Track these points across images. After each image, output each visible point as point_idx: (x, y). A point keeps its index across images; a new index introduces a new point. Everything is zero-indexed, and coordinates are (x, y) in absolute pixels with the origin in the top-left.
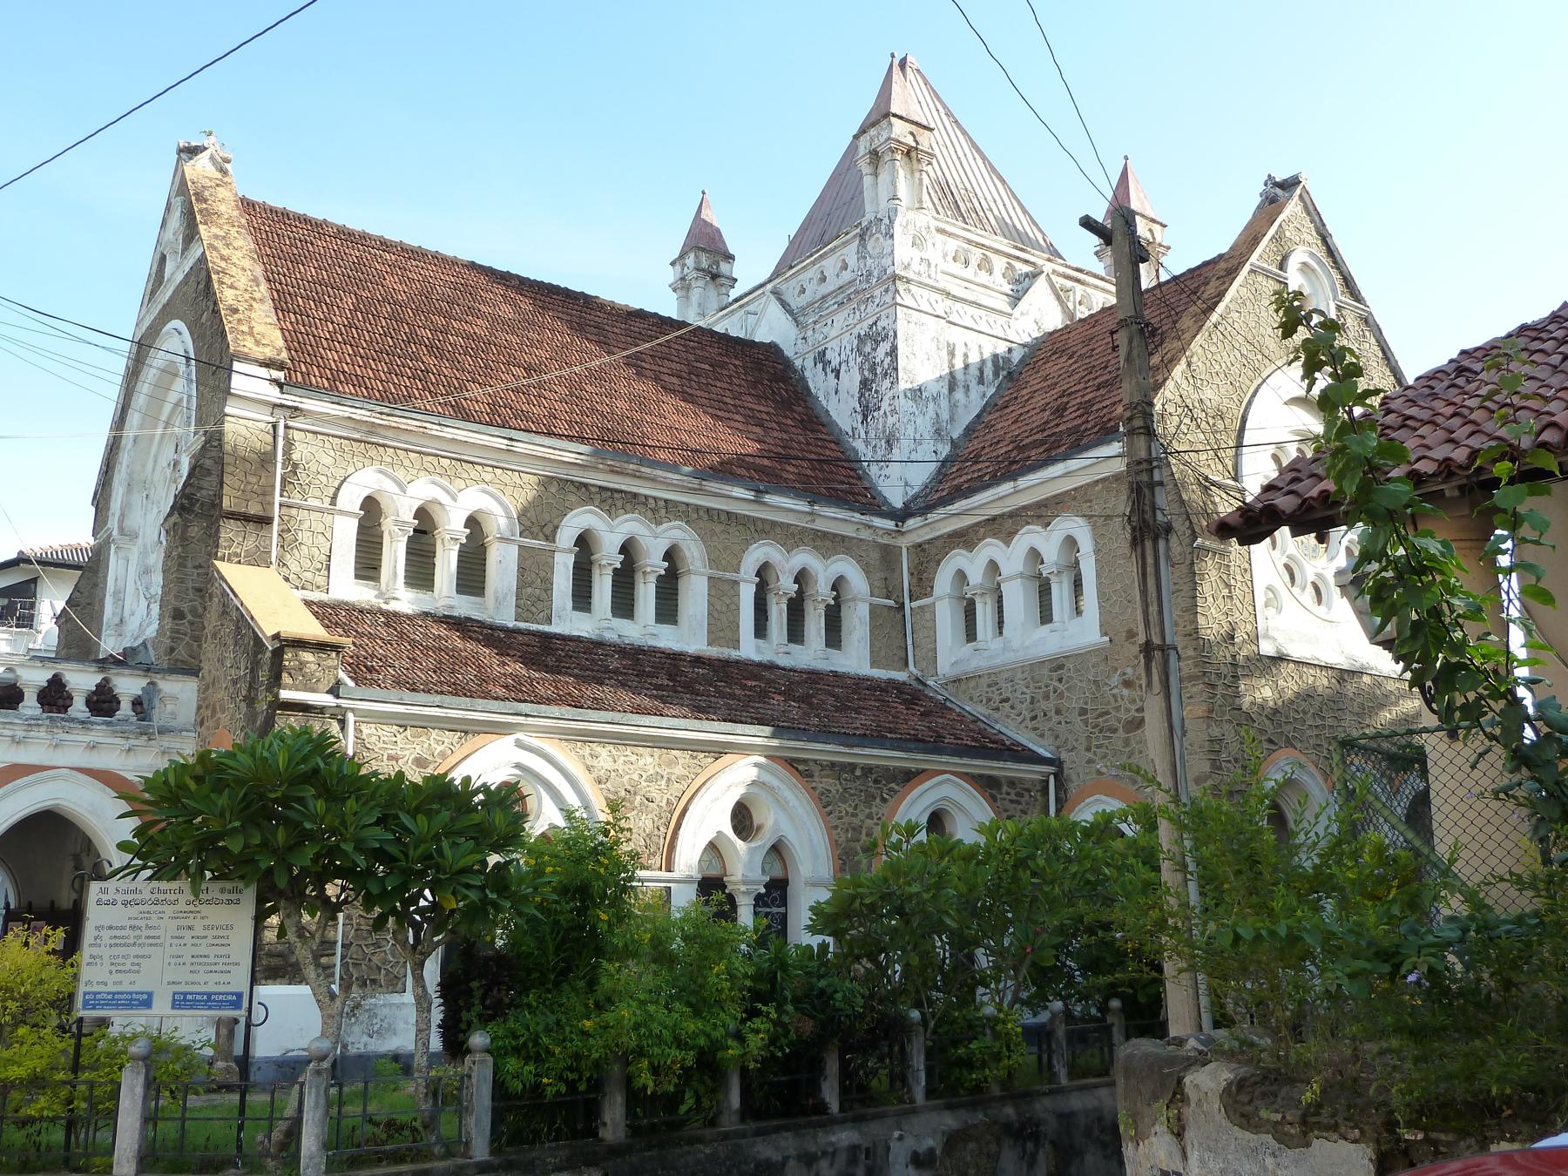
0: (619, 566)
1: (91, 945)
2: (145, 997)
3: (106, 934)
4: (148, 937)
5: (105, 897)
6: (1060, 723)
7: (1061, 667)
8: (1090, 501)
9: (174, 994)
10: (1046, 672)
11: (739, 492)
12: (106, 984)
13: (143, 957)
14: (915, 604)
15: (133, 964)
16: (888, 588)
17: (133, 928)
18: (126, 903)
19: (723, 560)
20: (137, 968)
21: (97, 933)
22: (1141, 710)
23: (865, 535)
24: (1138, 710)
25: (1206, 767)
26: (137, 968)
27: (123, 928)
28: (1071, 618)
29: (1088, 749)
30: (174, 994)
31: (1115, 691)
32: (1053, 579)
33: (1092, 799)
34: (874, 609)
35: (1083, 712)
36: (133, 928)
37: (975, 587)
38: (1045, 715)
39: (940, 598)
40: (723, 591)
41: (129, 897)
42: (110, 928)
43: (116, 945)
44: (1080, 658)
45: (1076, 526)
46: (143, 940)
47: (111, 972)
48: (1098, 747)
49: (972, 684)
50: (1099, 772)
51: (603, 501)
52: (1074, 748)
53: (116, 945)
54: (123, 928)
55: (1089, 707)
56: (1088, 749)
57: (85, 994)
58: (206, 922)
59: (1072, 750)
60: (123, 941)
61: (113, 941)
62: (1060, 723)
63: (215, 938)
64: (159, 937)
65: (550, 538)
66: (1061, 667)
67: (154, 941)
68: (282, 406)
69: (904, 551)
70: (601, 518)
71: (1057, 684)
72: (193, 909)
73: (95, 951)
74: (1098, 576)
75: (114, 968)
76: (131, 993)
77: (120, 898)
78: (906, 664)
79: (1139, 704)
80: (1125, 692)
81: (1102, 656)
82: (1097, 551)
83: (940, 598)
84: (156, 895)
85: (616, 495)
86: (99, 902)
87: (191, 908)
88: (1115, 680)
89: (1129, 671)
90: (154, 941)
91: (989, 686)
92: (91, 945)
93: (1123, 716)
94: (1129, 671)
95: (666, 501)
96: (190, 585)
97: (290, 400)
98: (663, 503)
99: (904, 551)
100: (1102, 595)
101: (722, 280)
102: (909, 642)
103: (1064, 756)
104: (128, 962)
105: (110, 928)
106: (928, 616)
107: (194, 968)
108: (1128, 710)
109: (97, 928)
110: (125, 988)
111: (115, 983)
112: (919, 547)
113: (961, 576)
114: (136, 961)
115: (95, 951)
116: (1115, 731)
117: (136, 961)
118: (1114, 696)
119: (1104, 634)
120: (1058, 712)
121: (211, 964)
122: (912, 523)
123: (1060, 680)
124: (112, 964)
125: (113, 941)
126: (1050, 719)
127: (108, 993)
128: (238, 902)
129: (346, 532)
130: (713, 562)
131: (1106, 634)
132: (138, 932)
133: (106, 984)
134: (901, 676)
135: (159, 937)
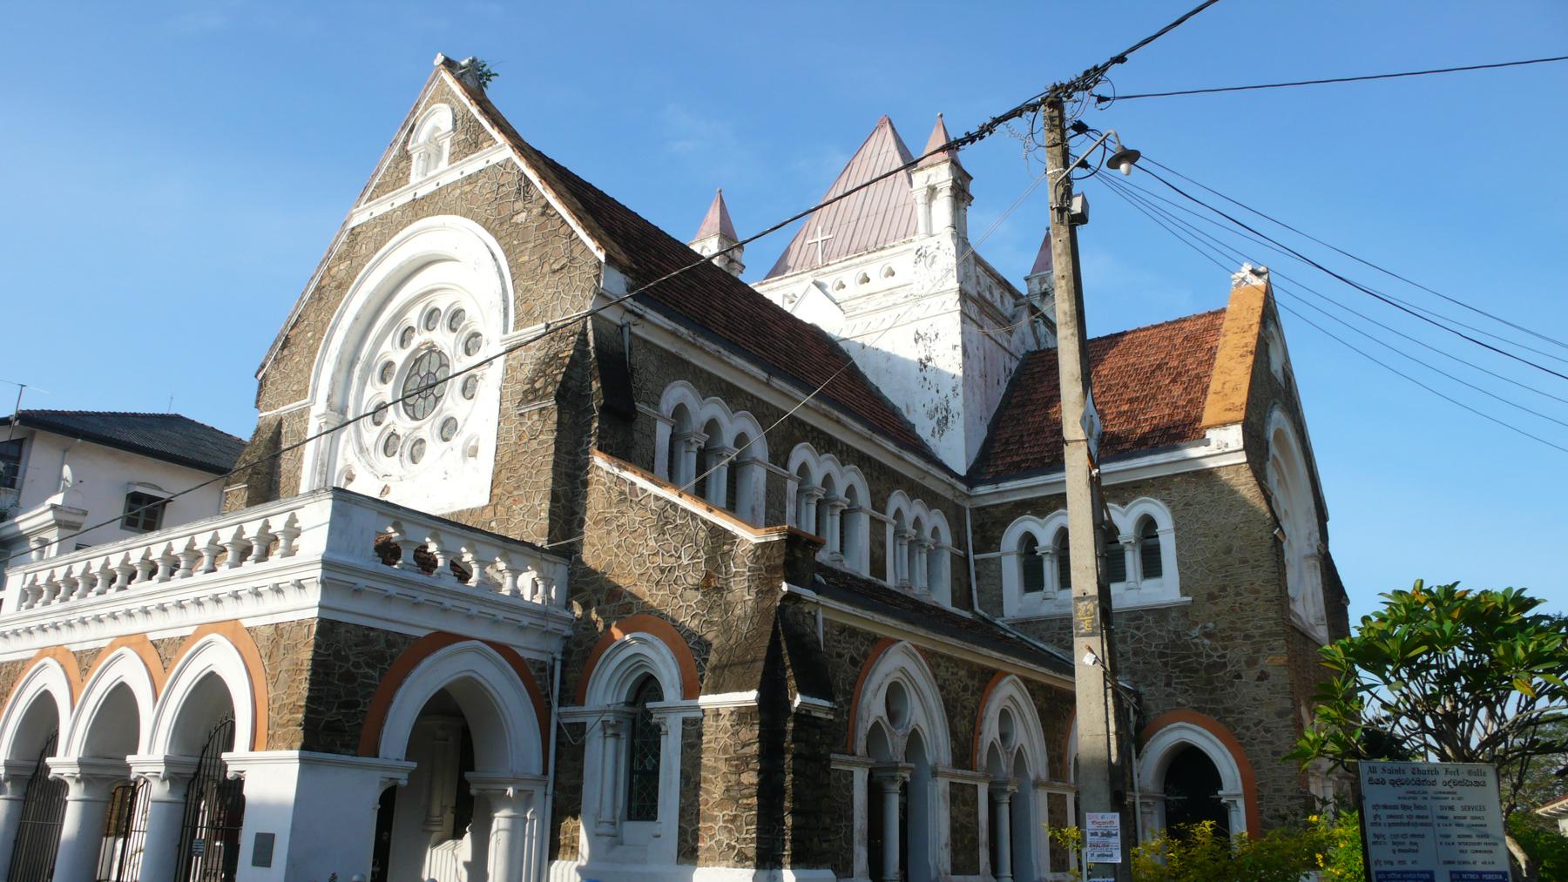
0: (822, 497)
1: (1373, 824)
2: (1428, 876)
3: (1383, 813)
4: (1418, 817)
5: (1375, 777)
6: (1138, 663)
7: (1140, 618)
8: (1169, 489)
9: (1452, 873)
10: (1123, 622)
11: (891, 446)
12: (1392, 863)
13: (1419, 836)
14: (978, 556)
15: (1411, 843)
16: (959, 541)
17: (1405, 807)
18: (1393, 783)
19: (879, 503)
20: (1415, 847)
21: (1374, 812)
22: (1223, 656)
23: (949, 495)
24: (1219, 657)
25: (1288, 704)
26: (1415, 847)
27: (1395, 807)
28: (1142, 580)
29: (1168, 685)
30: (1452, 873)
31: (1196, 640)
32: (1128, 547)
33: (1169, 727)
34: (953, 555)
35: (1162, 655)
36: (1405, 807)
37: (1046, 547)
38: (1122, 655)
39: (1007, 554)
40: (877, 525)
41: (1395, 777)
42: (1385, 807)
43: (1394, 824)
44: (1160, 613)
45: (1154, 507)
46: (1414, 820)
47: (1394, 851)
48: (1176, 683)
49: (1041, 626)
50: (1178, 704)
51: (814, 438)
52: (1153, 684)
53: (1394, 824)
54: (1395, 807)
55: (1168, 651)
56: (1168, 685)
57: (1378, 873)
58: (1463, 803)
59: (1151, 685)
60: (1399, 821)
61: (1391, 821)
62: (1138, 663)
63: (1473, 818)
64: (1427, 817)
65: (785, 467)
66: (1140, 618)
67: (1424, 821)
68: (632, 312)
69: (968, 512)
70: (813, 454)
71: (1136, 632)
72: (1451, 790)
73: (1378, 830)
74: (1178, 548)
75: (1396, 847)
76: (1416, 872)
77: (1388, 777)
78: (969, 606)
79: (1221, 652)
80: (1206, 641)
81: (1183, 610)
82: (1177, 529)
83: (1007, 554)
84: (1418, 776)
85: (821, 436)
86: (1371, 781)
87: (1447, 789)
88: (1196, 632)
89: (1211, 625)
90: (1424, 821)
91: (1060, 629)
92: (1373, 824)
93: (1204, 660)
94: (1211, 625)
95: (848, 446)
96: (563, 470)
97: (639, 307)
98: (845, 448)
99: (968, 512)
100: (1182, 564)
101: (736, 265)
102: (974, 587)
103: (1142, 689)
104: (1407, 841)
105: (1385, 807)
106: (993, 567)
107: (1462, 847)
108: (1209, 656)
109: (1376, 807)
110: (1409, 866)
111: (1400, 862)
112: (979, 511)
113: (1029, 541)
114: (1413, 840)
115: (1378, 830)
116: (1196, 671)
117: (1413, 840)
118: (1195, 644)
119: (1184, 594)
120: (1135, 654)
121: (1474, 844)
122: (981, 490)
123: (1138, 629)
124: (1394, 843)
125: (1391, 821)
126: (1128, 659)
127: (1398, 872)
128: (1484, 784)
129: (663, 432)
130: (874, 507)
131: (1186, 595)
132: (1408, 812)
133: (1392, 863)
134: (967, 614)
135: (1427, 817)
